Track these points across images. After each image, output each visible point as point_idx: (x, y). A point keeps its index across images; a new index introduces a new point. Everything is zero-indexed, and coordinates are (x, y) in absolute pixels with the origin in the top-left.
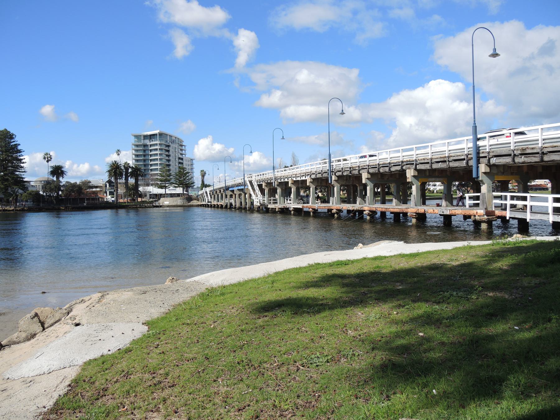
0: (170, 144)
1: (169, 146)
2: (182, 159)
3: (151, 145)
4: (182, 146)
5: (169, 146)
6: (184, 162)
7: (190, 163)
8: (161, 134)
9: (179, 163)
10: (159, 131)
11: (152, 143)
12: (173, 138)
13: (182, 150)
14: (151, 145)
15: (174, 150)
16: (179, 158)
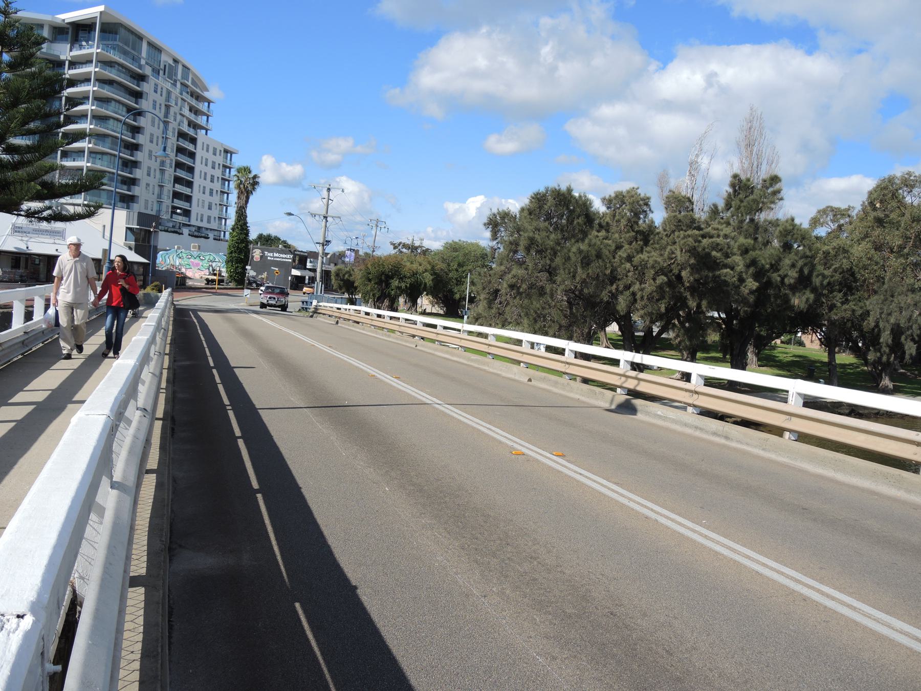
0: (148, 71)
1: (141, 78)
2: (193, 141)
3: (73, 64)
4: (198, 98)
5: (141, 78)
6: (200, 153)
7: (219, 159)
8: (111, 29)
9: (180, 150)
10: (101, 8)
11: (76, 53)
12: (164, 58)
13: (196, 112)
14: (73, 64)
15: (161, 100)
16: (182, 135)
